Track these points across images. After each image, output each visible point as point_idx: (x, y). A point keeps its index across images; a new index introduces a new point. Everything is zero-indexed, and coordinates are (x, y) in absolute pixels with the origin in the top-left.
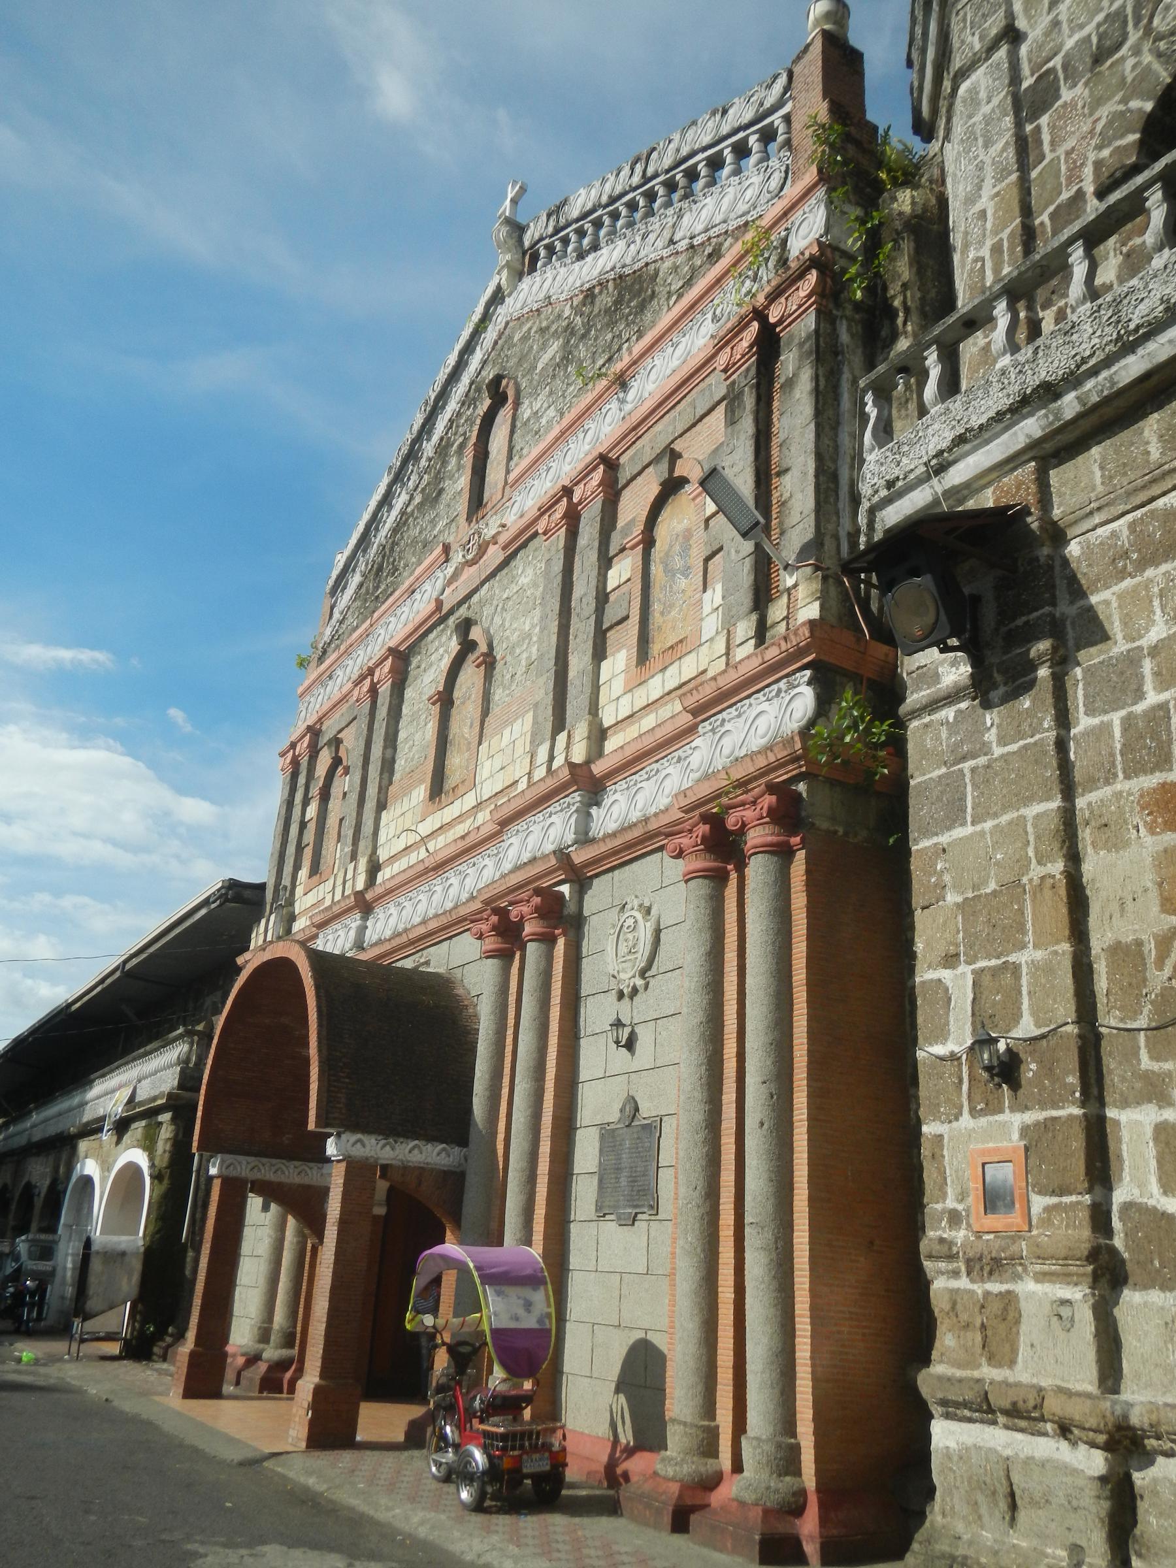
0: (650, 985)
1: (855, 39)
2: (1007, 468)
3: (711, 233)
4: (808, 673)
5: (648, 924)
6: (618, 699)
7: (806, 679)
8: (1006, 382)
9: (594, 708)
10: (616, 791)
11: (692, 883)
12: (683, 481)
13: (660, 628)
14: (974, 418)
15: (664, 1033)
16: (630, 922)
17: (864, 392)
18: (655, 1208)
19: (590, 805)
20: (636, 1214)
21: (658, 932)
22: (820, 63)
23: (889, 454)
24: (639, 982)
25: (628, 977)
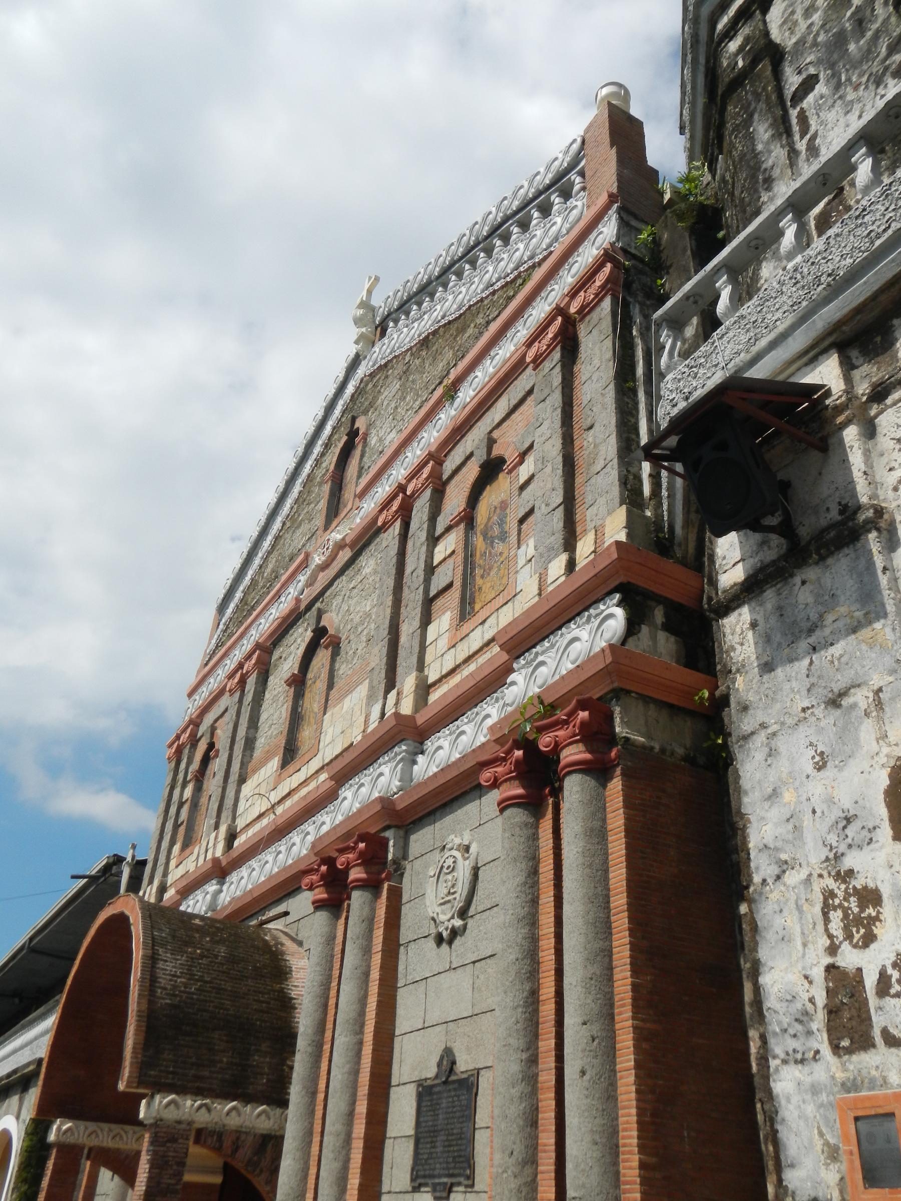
0: (469, 926)
1: (635, 111)
2: (805, 359)
3: (522, 269)
4: (617, 596)
5: (467, 862)
6: (442, 655)
7: (615, 601)
8: (799, 276)
9: (421, 665)
10: (439, 738)
11: (508, 812)
12: (501, 461)
13: (480, 589)
14: (769, 316)
15: (482, 977)
16: (450, 862)
17: (659, 325)
18: (471, 1177)
19: (416, 754)
20: (452, 1185)
21: (476, 872)
22: (607, 124)
23: (686, 370)
24: (458, 923)
25: (447, 919)
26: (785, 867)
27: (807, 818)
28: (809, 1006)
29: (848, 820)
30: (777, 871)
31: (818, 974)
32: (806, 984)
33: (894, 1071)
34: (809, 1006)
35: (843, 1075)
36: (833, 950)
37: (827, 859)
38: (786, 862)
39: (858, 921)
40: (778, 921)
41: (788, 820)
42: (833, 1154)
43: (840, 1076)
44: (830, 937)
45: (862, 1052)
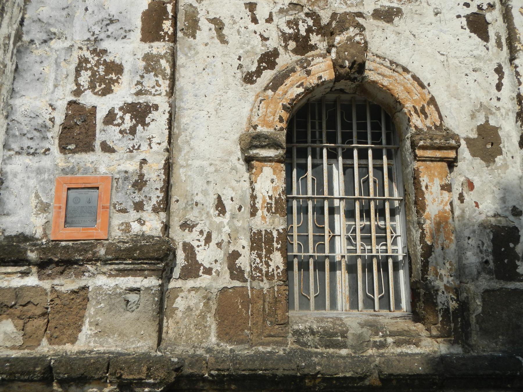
26: (53, 36)
27: (79, 13)
28: (49, 123)
29: (112, 21)
30: (45, 37)
31: (62, 105)
32: (50, 110)
33: (104, 165)
34: (49, 123)
35: (64, 164)
36: (78, 92)
37: (89, 40)
38: (55, 34)
39: (102, 80)
40: (38, 68)
41: (64, 9)
42: (44, 208)
43: (62, 164)
44: (78, 85)
45: (83, 153)
